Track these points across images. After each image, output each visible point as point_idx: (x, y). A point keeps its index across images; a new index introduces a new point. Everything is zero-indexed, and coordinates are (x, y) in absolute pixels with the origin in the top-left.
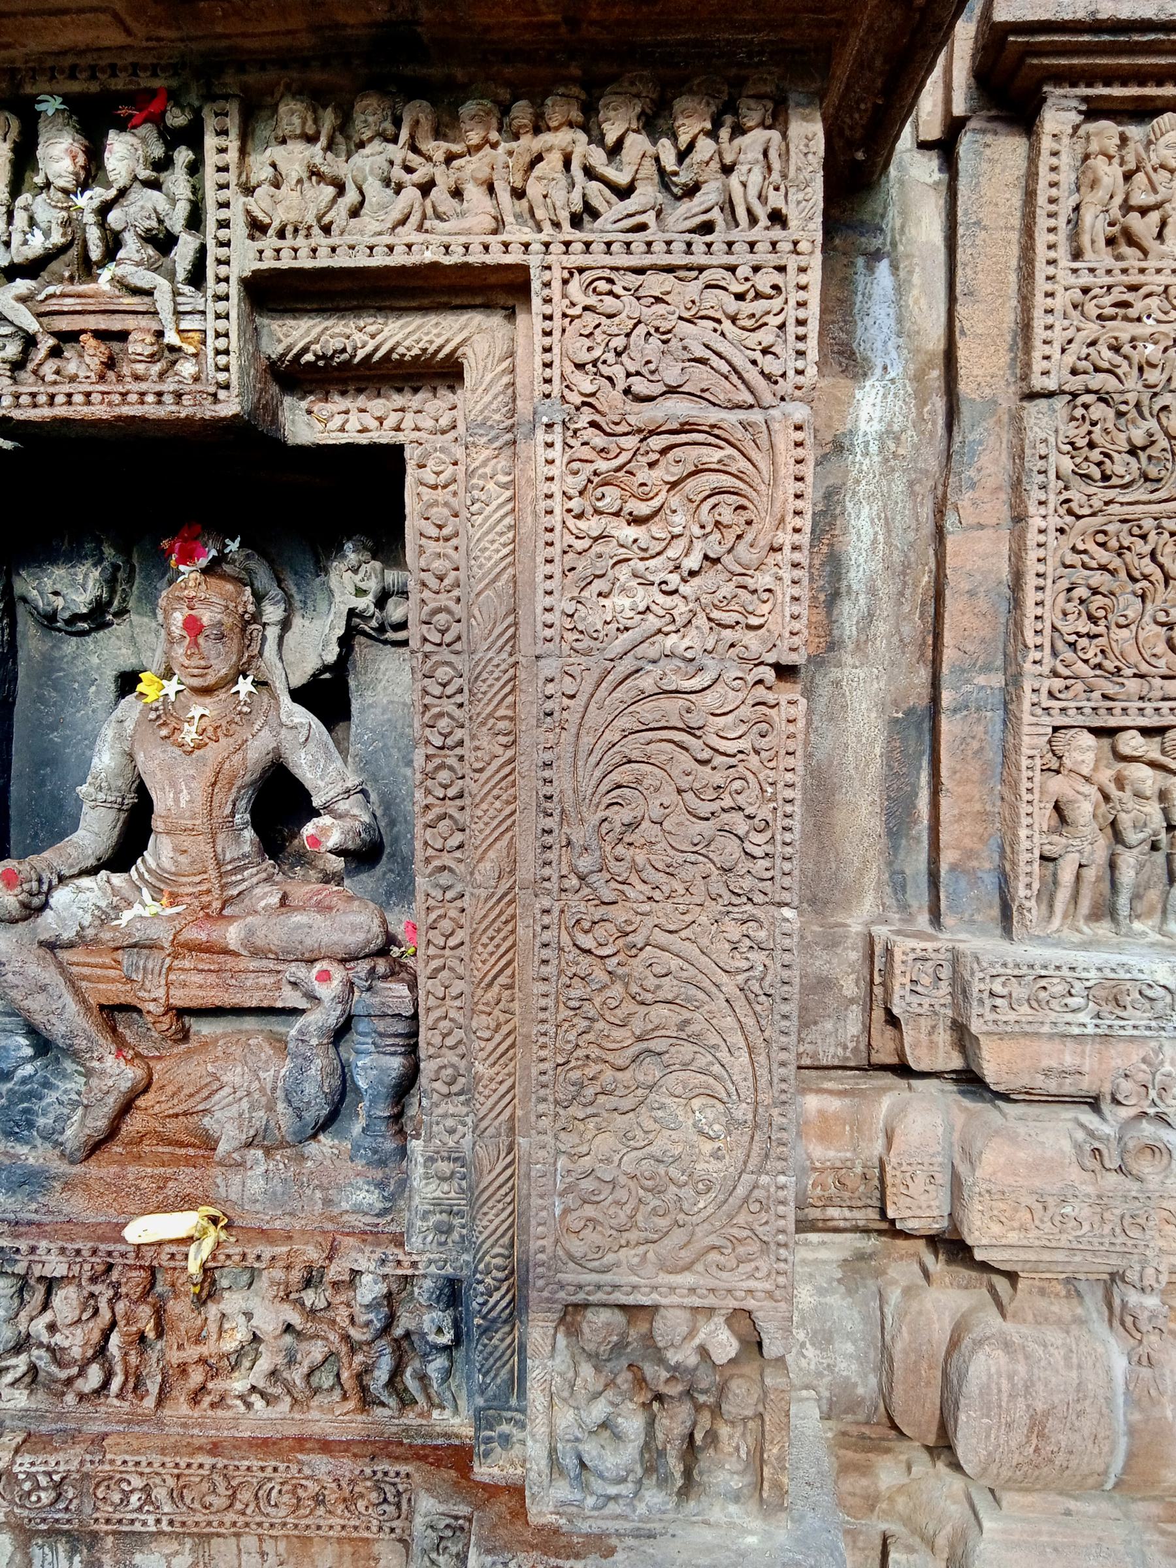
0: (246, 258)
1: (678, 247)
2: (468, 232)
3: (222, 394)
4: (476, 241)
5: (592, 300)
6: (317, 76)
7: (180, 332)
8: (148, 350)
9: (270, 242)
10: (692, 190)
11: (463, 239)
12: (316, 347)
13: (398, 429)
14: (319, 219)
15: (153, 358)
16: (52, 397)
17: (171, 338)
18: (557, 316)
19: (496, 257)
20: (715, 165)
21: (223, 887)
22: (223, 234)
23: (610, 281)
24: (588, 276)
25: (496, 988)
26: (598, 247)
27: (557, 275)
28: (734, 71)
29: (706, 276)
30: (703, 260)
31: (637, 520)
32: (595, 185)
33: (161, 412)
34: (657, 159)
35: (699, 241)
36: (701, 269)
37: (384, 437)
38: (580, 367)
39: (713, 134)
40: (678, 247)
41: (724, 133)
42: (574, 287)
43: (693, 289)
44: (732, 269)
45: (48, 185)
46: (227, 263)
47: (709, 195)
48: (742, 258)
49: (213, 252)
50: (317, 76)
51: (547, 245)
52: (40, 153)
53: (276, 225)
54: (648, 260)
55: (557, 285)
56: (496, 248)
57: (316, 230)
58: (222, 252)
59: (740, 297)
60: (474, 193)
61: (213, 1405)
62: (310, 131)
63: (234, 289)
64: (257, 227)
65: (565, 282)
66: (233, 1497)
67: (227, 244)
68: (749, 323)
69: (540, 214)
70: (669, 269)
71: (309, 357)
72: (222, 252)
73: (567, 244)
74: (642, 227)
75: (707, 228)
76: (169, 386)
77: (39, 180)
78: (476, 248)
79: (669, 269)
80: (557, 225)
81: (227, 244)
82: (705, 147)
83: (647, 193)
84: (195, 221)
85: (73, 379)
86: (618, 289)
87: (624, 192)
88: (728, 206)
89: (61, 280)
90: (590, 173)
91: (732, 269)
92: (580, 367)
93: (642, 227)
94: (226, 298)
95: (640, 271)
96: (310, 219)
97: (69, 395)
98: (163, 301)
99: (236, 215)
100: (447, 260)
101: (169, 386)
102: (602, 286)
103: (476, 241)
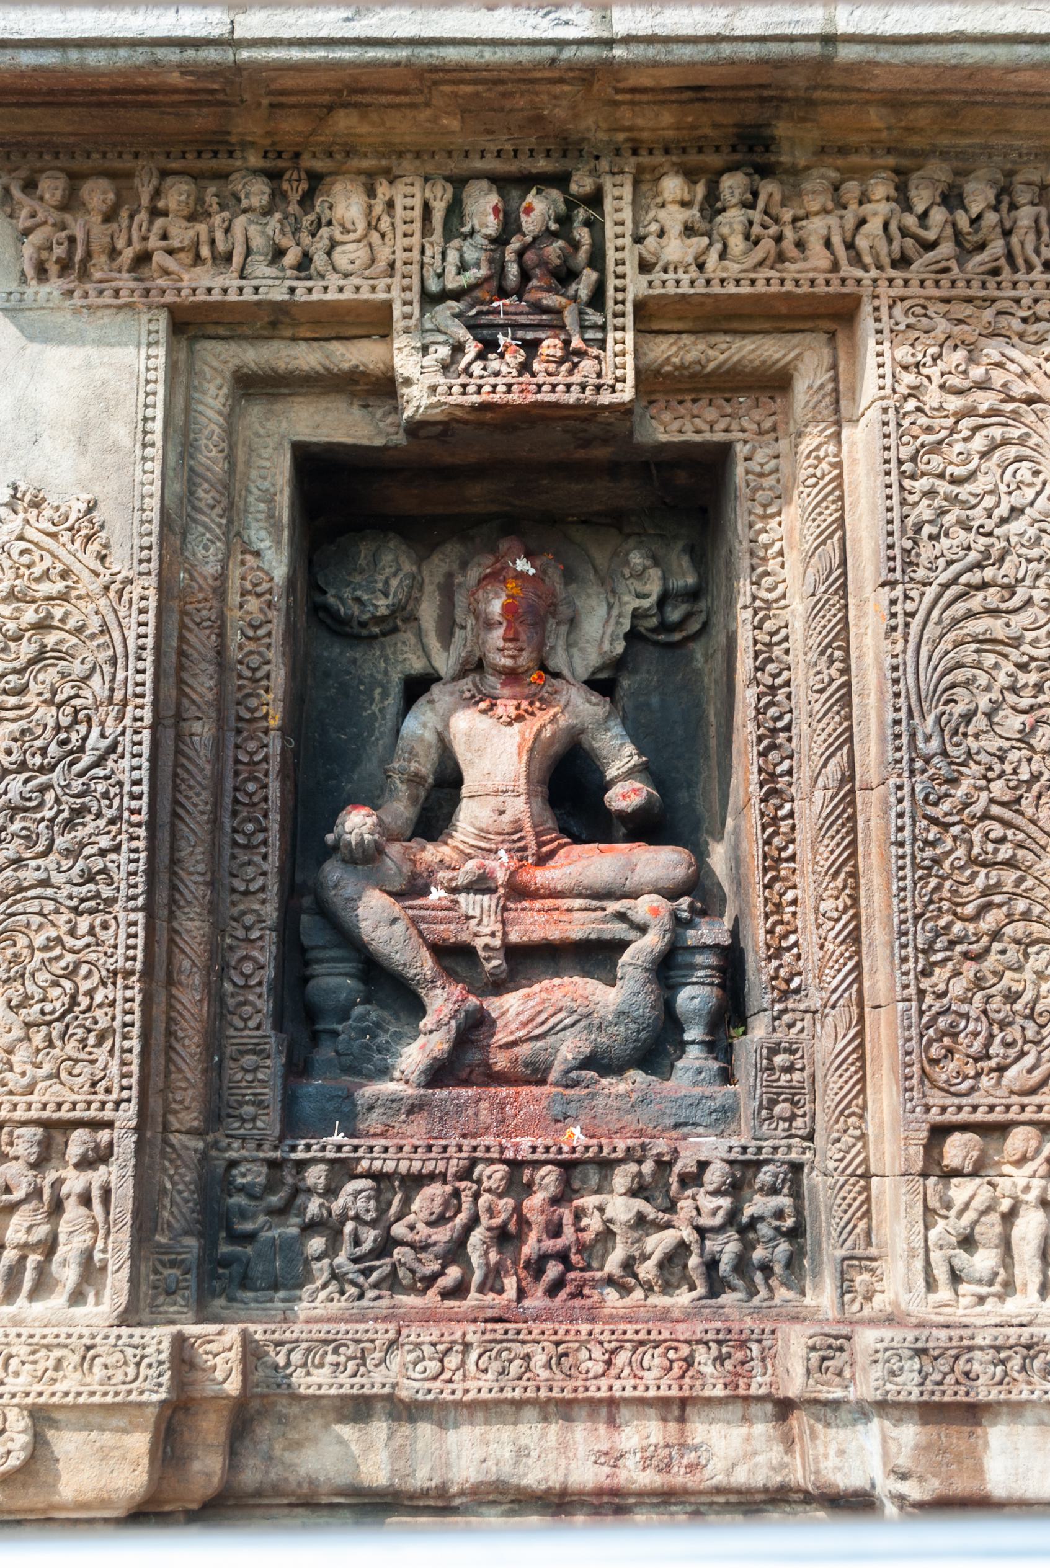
0: (636, 286)
1: (975, 284)
2: (815, 270)
3: (619, 386)
4: (821, 278)
5: (912, 320)
6: (693, 159)
7: (585, 340)
8: (559, 353)
9: (657, 275)
10: (982, 247)
11: (811, 275)
12: (676, 360)
13: (726, 431)
14: (696, 259)
15: (561, 362)
16: (480, 387)
17: (576, 343)
18: (887, 331)
19: (835, 288)
20: (998, 230)
21: (540, 845)
22: (620, 269)
23: (924, 307)
24: (907, 303)
25: (842, 875)
26: (915, 283)
27: (884, 303)
28: (1009, 166)
29: (998, 305)
30: (997, 293)
31: (955, 481)
32: (909, 241)
33: (571, 398)
34: (954, 225)
35: (991, 282)
36: (994, 301)
37: (719, 437)
38: (905, 368)
39: (996, 208)
40: (975, 284)
41: (1004, 207)
42: (898, 311)
43: (988, 314)
44: (1018, 301)
45: (473, 233)
46: (623, 290)
47: (997, 247)
48: (1022, 292)
49: (611, 283)
50: (693, 159)
51: (875, 281)
52: (468, 210)
53: (661, 264)
54: (954, 292)
55: (884, 311)
56: (836, 282)
57: (693, 268)
58: (619, 283)
59: (1025, 320)
60: (815, 246)
61: (572, 1296)
62: (687, 197)
63: (629, 308)
64: (645, 267)
65: (890, 307)
66: (609, 1363)
67: (623, 277)
68: (1033, 339)
69: (868, 259)
70: (969, 300)
71: (668, 368)
72: (619, 283)
73: (891, 281)
74: (946, 270)
75: (995, 272)
76: (576, 378)
77: (466, 229)
78: (821, 281)
79: (969, 300)
80: (880, 267)
81: (623, 277)
82: (991, 218)
83: (946, 248)
84: (597, 260)
85: (497, 374)
86: (930, 313)
87: (930, 246)
88: (1010, 256)
89: (482, 303)
90: (904, 232)
91: (1018, 301)
92: (905, 368)
93: (946, 270)
94: (623, 315)
95: (947, 301)
96: (690, 259)
97: (495, 386)
98: (570, 318)
99: (631, 257)
100: (799, 291)
101: (576, 378)
102: (919, 310)
103: (821, 278)
